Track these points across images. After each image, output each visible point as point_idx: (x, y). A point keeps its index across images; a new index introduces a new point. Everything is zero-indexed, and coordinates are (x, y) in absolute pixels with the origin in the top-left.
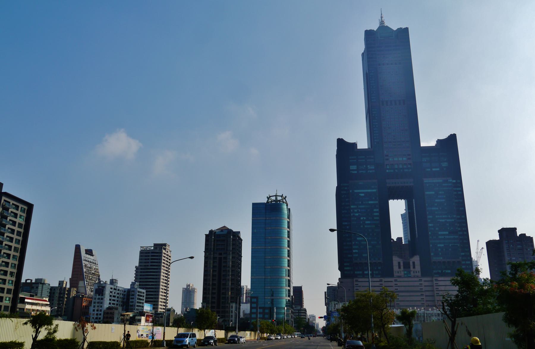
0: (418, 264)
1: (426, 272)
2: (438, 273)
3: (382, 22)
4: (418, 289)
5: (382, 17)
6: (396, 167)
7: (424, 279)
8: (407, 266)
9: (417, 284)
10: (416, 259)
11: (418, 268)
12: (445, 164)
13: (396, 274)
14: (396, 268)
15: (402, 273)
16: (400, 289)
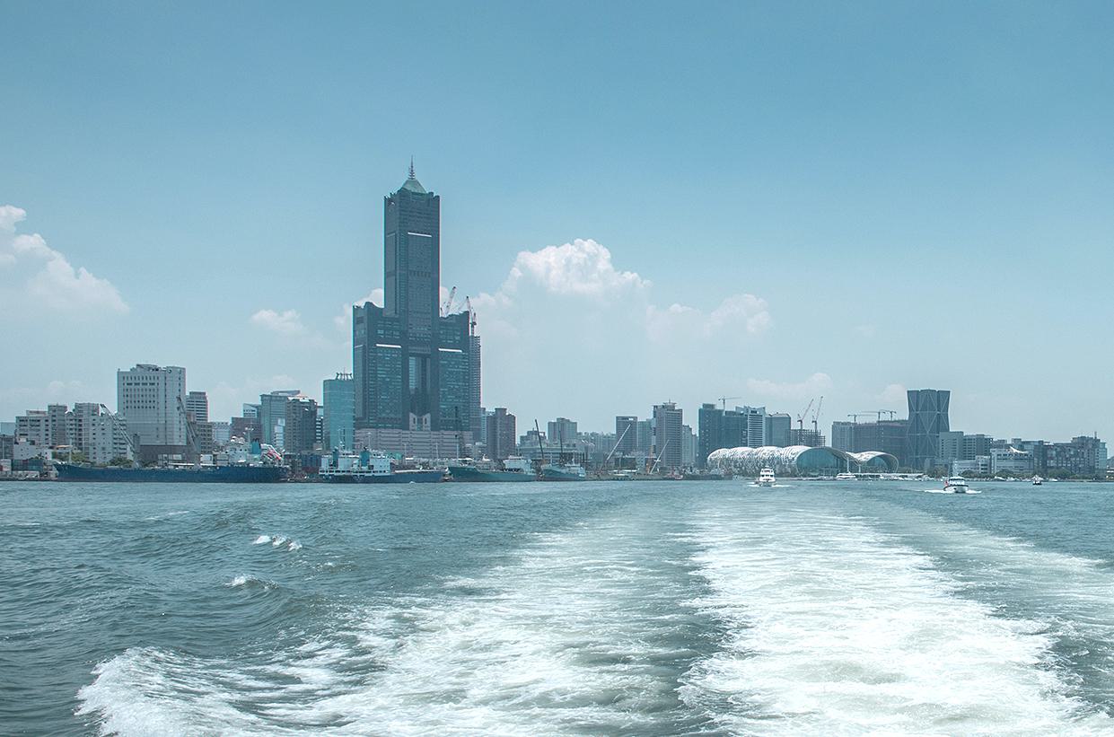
0: (429, 420)
1: (435, 427)
2: (443, 429)
3: (412, 180)
4: (427, 440)
5: (412, 173)
6: (418, 335)
7: (432, 432)
8: (420, 421)
9: (428, 436)
10: (428, 416)
11: (429, 424)
12: (457, 338)
13: (411, 428)
14: (411, 423)
15: (416, 428)
16: (414, 440)
